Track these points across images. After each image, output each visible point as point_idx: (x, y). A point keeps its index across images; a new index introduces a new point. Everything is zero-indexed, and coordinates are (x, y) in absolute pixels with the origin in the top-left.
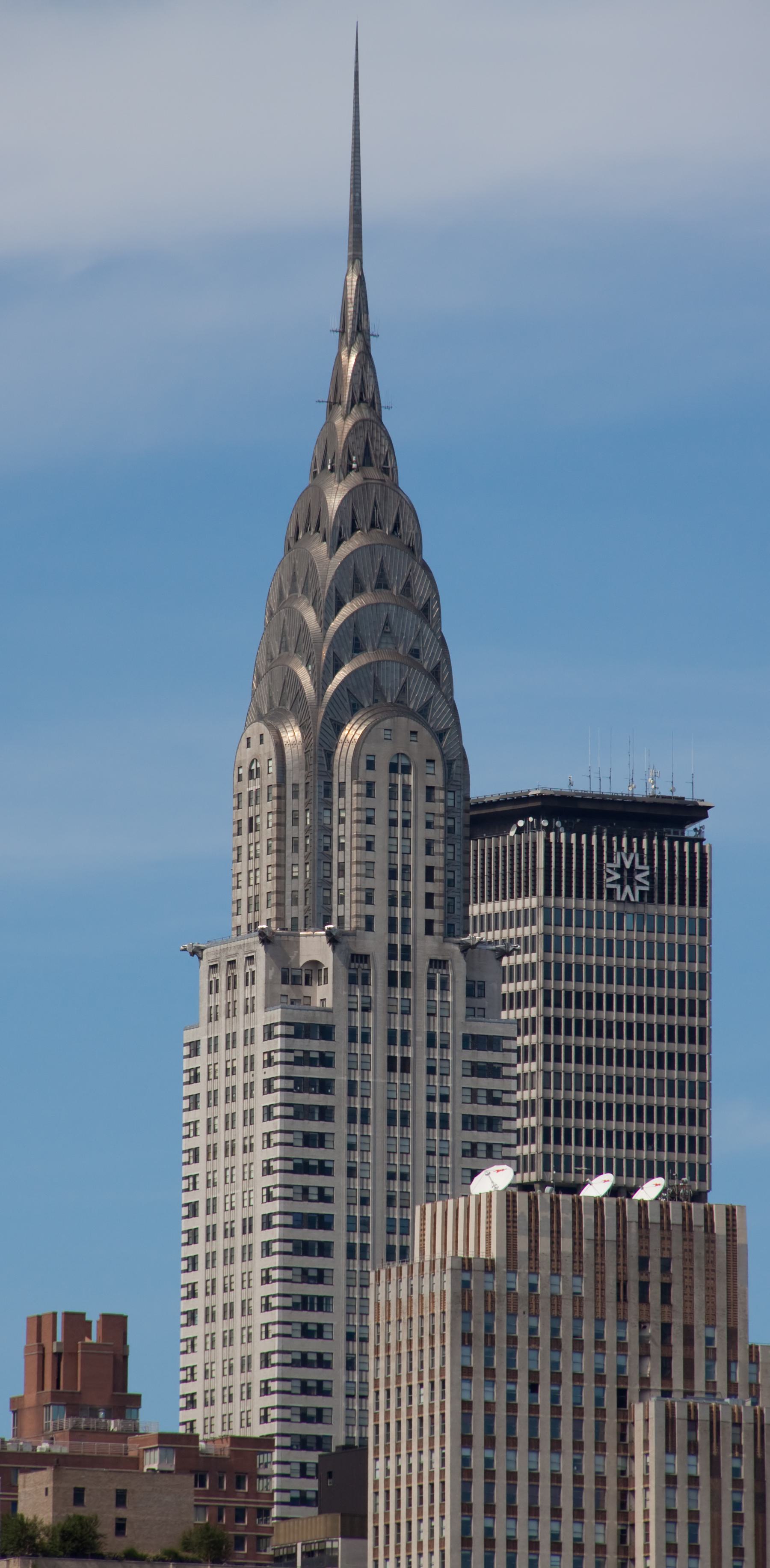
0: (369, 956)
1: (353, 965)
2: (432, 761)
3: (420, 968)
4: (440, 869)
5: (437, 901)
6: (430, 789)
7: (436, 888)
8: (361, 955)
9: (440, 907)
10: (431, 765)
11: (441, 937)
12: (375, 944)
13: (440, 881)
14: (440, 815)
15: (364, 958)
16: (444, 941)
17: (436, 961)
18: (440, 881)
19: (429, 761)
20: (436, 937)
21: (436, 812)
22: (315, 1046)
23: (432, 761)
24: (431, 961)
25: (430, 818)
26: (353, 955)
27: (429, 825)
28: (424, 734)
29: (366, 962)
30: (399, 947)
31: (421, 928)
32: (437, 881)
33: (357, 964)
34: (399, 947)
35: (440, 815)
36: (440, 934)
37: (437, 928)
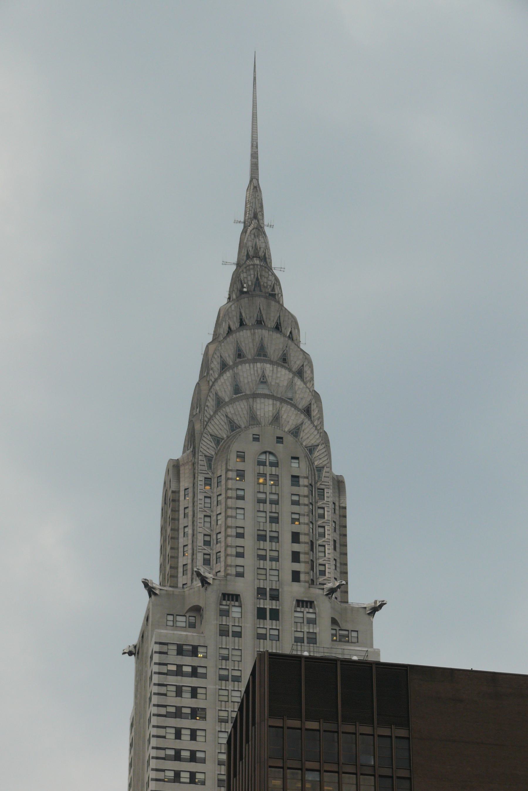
0: (239, 595)
1: (224, 603)
2: (297, 458)
3: (287, 604)
4: (305, 534)
6: (295, 480)
8: (233, 595)
9: (305, 562)
10: (297, 461)
11: (307, 585)
12: (245, 587)
13: (305, 543)
14: (305, 496)
15: (235, 597)
17: (303, 601)
18: (305, 543)
19: (293, 458)
21: (300, 493)
22: (188, 661)
23: (297, 458)
24: (298, 601)
25: (296, 498)
26: (224, 595)
27: (294, 503)
28: (289, 439)
29: (237, 601)
30: (268, 590)
31: (289, 577)
32: (302, 543)
33: (228, 602)
34: (268, 590)
35: (305, 496)
36: (305, 582)
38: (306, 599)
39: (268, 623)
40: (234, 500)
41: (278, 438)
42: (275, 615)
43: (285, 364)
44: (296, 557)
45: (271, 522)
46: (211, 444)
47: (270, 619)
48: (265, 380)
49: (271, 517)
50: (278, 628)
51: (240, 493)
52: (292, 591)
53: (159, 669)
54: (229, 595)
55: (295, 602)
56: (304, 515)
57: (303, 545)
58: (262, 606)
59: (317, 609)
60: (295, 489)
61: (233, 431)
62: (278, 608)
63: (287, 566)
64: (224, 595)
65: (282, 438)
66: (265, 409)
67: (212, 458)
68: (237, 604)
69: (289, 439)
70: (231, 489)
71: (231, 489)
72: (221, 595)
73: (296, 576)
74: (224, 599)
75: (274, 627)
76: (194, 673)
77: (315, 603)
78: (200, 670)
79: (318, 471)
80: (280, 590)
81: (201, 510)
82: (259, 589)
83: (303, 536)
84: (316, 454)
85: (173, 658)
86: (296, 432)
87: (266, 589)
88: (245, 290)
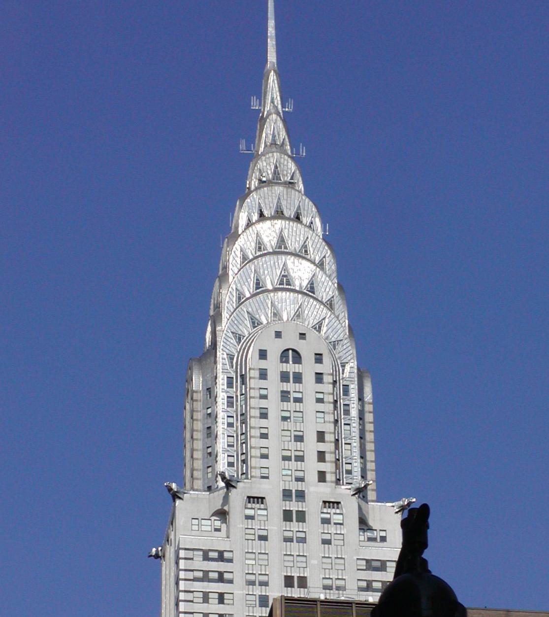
3: (313, 507)
4: (330, 433)
5: (328, 457)
7: (327, 447)
8: (258, 498)
9: (331, 462)
11: (334, 485)
12: (272, 490)
13: (331, 442)
15: (261, 500)
16: (335, 488)
20: (329, 484)
25: (320, 396)
29: (262, 503)
30: (294, 491)
32: (328, 442)
34: (294, 491)
35: (329, 394)
36: (332, 482)
37: (330, 477)
38: (332, 500)
39: (295, 526)
40: (257, 400)
41: (301, 334)
42: (301, 516)
43: (306, 256)
44: (321, 457)
45: (295, 441)
46: (232, 341)
47: (297, 521)
48: (286, 274)
49: (295, 436)
50: (304, 530)
51: (263, 392)
52: (317, 492)
53: (185, 575)
54: (254, 498)
55: (321, 503)
56: (329, 413)
57: (328, 444)
58: (288, 508)
59: (344, 509)
60: (320, 388)
61: (254, 327)
62: (304, 510)
63: (312, 467)
64: (249, 497)
65: (304, 334)
66: (287, 303)
67: (234, 356)
68: (262, 506)
69: (312, 335)
70: (254, 389)
71: (254, 389)
72: (246, 498)
73: (322, 476)
74: (249, 502)
75: (301, 530)
76: (221, 579)
77: (342, 503)
78: (226, 576)
79: (342, 366)
80: (306, 492)
81: (224, 410)
82: (284, 490)
83: (328, 435)
84: (339, 348)
85: (199, 564)
86: (318, 327)
87: (291, 490)
88: (264, 179)
